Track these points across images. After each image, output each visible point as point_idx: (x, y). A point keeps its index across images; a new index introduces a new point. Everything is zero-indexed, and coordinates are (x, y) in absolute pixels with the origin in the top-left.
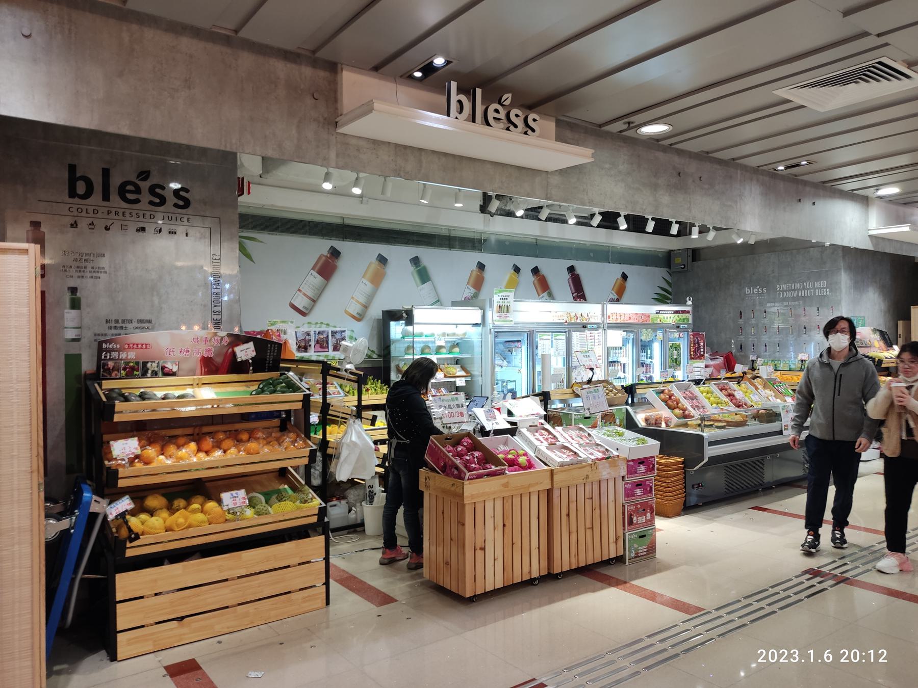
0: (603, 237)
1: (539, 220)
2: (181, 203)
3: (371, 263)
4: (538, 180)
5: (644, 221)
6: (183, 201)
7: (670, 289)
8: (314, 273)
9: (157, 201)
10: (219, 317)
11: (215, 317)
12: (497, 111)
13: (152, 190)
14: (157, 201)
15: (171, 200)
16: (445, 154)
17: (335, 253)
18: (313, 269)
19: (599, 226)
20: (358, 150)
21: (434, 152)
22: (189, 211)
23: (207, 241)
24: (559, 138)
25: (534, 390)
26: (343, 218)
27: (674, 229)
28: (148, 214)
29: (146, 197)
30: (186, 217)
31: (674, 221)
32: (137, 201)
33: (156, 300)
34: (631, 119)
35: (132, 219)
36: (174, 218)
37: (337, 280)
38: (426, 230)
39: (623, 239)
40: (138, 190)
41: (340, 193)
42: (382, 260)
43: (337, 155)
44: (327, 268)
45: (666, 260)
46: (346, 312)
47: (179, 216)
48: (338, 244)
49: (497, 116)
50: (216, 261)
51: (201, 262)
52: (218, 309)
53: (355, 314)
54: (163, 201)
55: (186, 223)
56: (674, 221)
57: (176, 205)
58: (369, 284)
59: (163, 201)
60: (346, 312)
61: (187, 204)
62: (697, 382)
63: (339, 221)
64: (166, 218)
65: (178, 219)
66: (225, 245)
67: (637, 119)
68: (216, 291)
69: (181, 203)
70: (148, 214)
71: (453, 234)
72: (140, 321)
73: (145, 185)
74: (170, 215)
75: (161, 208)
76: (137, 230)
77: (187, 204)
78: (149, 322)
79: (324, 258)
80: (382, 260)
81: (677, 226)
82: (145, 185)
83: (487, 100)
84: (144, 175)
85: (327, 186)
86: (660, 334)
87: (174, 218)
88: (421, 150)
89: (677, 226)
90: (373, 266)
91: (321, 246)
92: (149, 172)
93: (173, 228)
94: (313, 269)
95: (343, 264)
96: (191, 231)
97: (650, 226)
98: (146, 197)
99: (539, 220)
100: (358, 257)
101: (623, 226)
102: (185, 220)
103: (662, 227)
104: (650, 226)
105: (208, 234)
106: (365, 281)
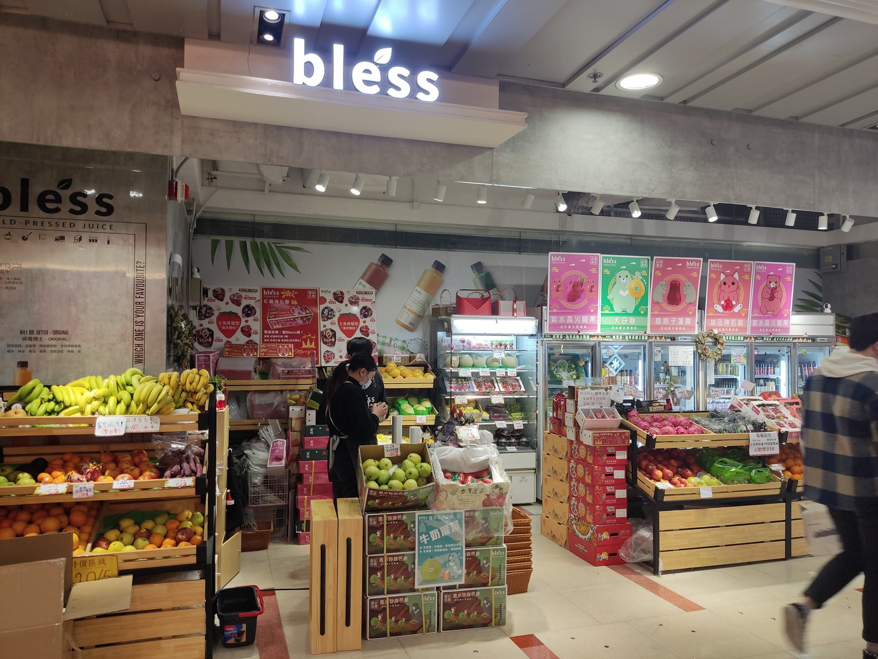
0: (691, 231)
1: (592, 214)
2: (104, 210)
3: (425, 271)
4: (477, 159)
5: (744, 211)
6: (106, 207)
7: (820, 295)
8: (364, 282)
9: (78, 209)
10: (141, 328)
11: (137, 328)
12: (367, 71)
13: (73, 199)
14: (78, 209)
15: (93, 207)
16: (338, 134)
17: (386, 261)
18: (362, 278)
19: (758, 225)
20: (212, 134)
21: (321, 132)
22: (112, 217)
23: (131, 249)
24: (502, 106)
25: (698, 408)
26: (396, 225)
27: (823, 225)
28: (68, 223)
29: (66, 205)
30: (108, 225)
31: (790, 210)
32: (57, 210)
33: (73, 310)
34: (598, 66)
35: (92, 230)
36: (95, 226)
37: (389, 289)
38: (491, 234)
39: (756, 238)
40: (58, 199)
41: (337, 194)
42: (439, 267)
43: (183, 142)
44: (377, 277)
45: (810, 260)
46: (398, 322)
47: (100, 224)
48: (390, 252)
49: (368, 77)
50: (139, 266)
51: (123, 268)
52: (142, 319)
53: (407, 324)
54: (84, 208)
55: (108, 230)
56: (790, 210)
57: (98, 213)
58: (423, 292)
59: (84, 208)
60: (398, 322)
61: (110, 210)
62: (268, 446)
63: (248, 219)
64: (87, 226)
65: (100, 226)
66: (152, 251)
67: (605, 67)
68: (140, 300)
69: (104, 210)
70: (68, 223)
71: (524, 236)
72: (56, 332)
73: (66, 194)
74: (91, 223)
75: (82, 217)
76: (56, 240)
77: (110, 210)
78: (65, 333)
79: (374, 267)
80: (439, 267)
81: (794, 215)
82: (66, 194)
83: (351, 58)
84: (66, 183)
85: (355, 192)
86: (785, 349)
87: (95, 226)
88: (301, 130)
89: (794, 215)
90: (428, 274)
91: (372, 254)
92: (71, 180)
93: (94, 236)
94: (362, 278)
95: (394, 272)
96: (112, 238)
97: (754, 217)
98: (66, 205)
99: (592, 214)
100: (412, 264)
101: (713, 219)
102: (108, 227)
103: (807, 221)
104: (754, 217)
105: (132, 241)
106: (419, 289)
